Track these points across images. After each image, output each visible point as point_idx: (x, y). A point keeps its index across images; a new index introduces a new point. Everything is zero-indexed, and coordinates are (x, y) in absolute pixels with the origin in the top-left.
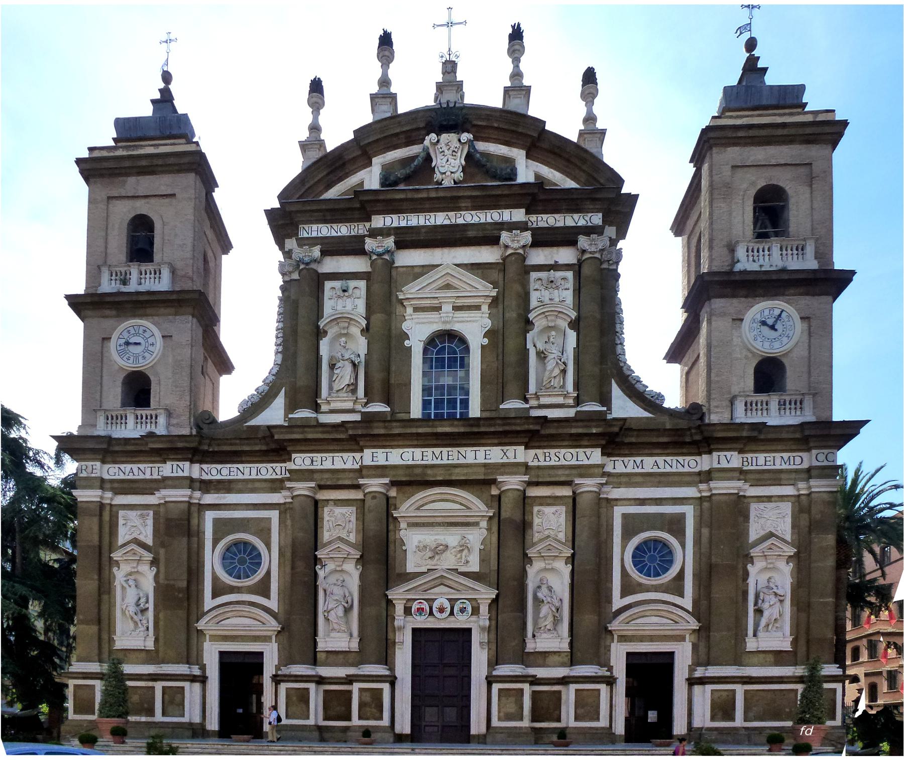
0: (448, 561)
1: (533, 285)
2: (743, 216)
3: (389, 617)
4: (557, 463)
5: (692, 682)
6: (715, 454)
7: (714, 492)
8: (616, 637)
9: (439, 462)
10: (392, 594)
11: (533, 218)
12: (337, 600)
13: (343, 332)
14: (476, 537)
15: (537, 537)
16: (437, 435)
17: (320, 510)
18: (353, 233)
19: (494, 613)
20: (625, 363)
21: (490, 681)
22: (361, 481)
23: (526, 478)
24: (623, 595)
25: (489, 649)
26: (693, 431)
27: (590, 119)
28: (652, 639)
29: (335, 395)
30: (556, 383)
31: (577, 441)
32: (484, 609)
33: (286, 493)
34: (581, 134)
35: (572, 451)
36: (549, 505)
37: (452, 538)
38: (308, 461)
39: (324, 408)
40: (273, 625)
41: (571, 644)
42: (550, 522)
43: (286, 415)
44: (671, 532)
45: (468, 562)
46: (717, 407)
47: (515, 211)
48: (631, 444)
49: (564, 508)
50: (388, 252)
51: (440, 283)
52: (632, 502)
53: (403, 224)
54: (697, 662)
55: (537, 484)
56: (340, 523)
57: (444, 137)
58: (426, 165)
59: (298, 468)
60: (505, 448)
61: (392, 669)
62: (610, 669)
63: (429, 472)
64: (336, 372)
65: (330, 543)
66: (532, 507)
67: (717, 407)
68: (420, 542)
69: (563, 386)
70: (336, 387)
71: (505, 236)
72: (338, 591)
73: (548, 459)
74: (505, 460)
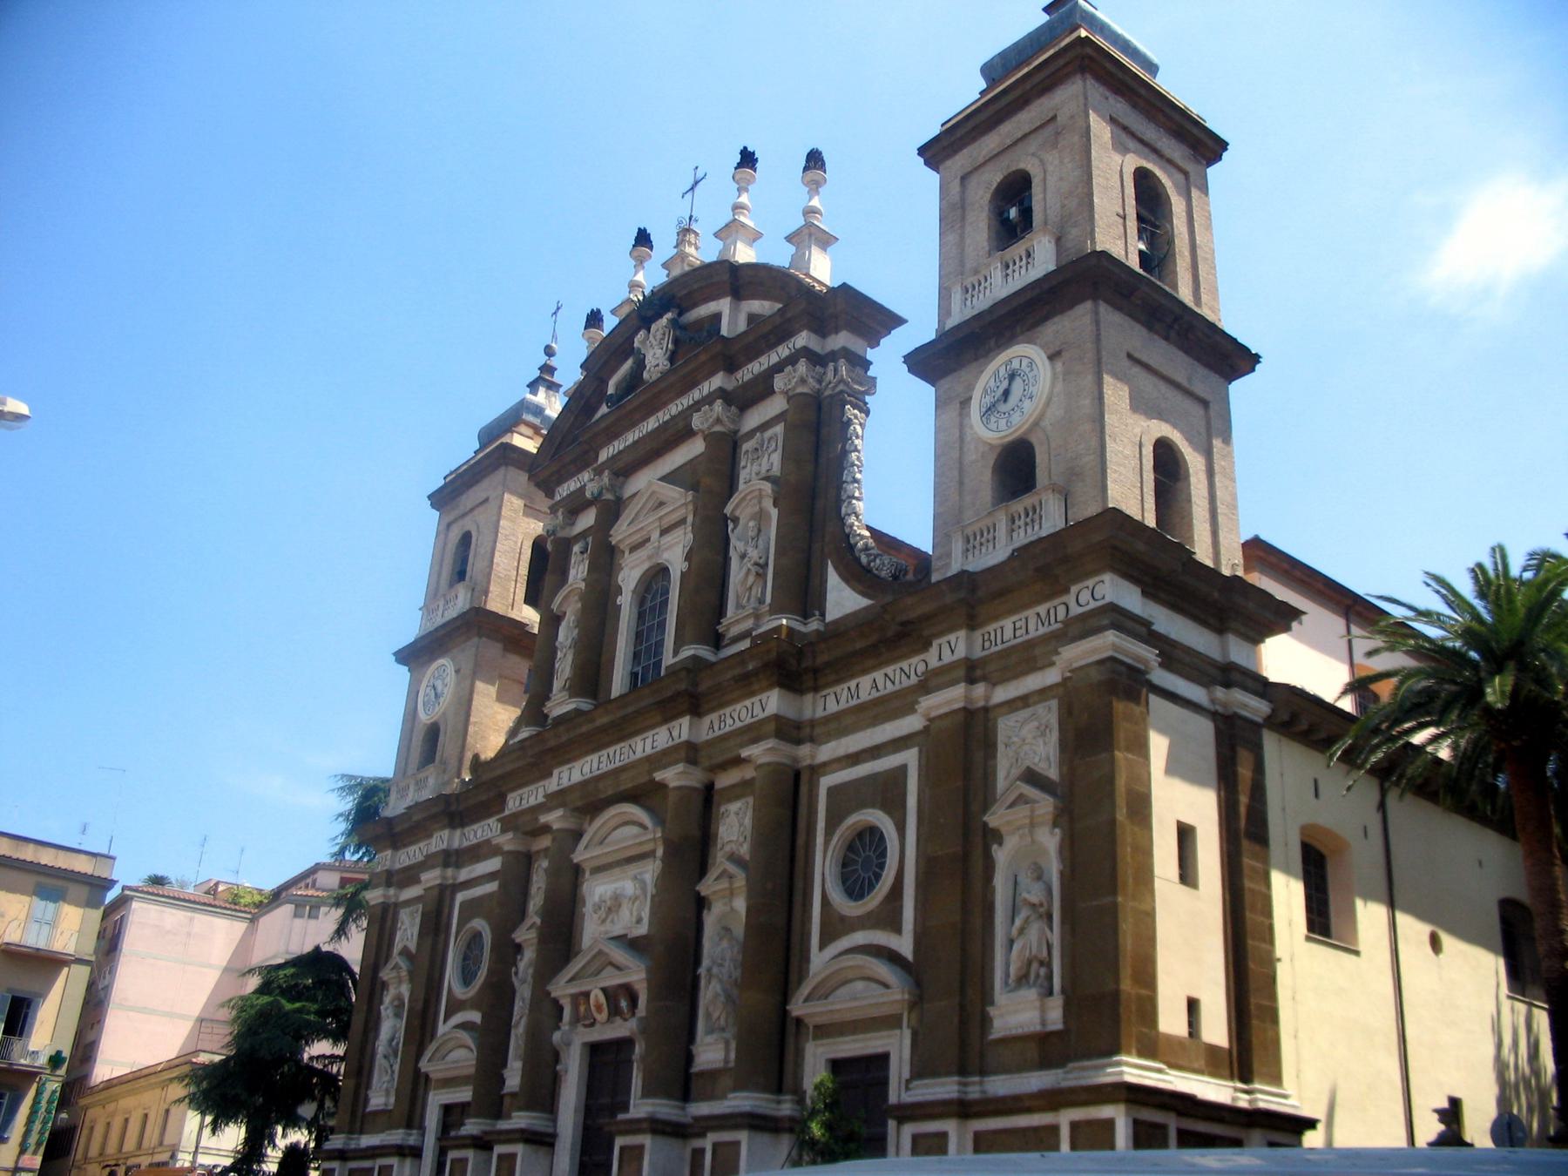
11: (739, 374)
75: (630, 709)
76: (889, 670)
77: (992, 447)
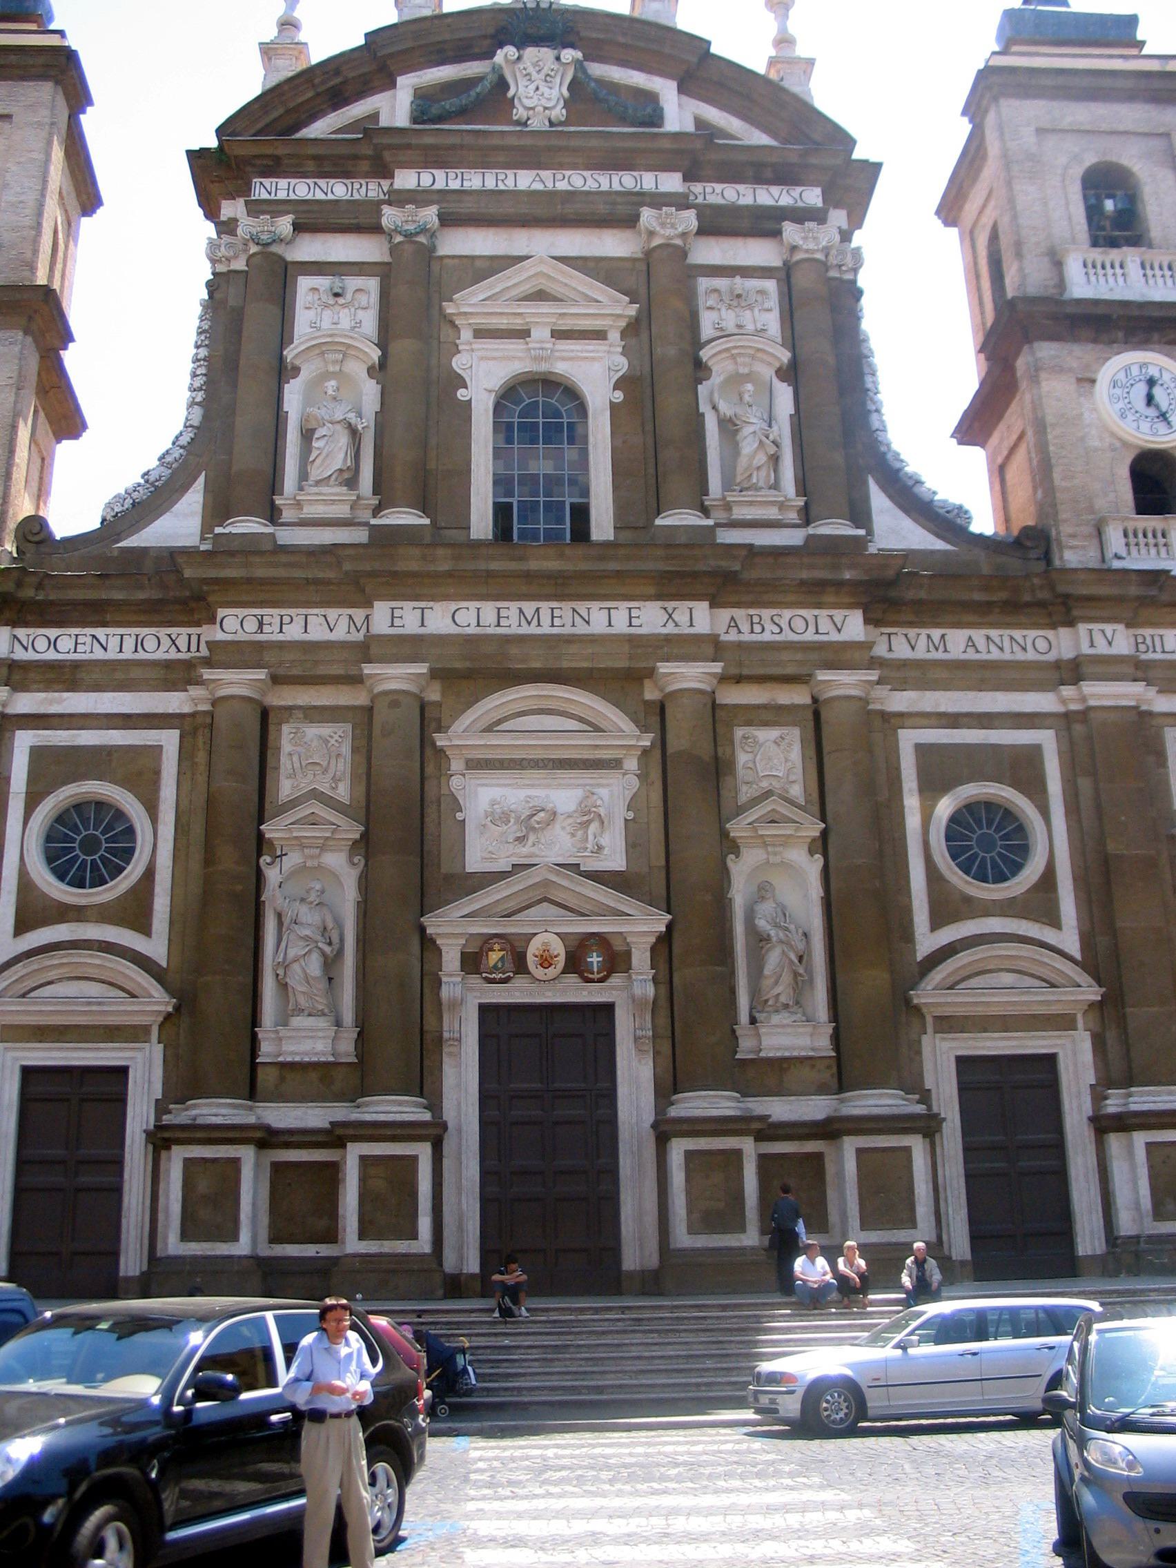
0: (558, 845)
1: (703, 301)
2: (1065, 212)
3: (431, 979)
4: (778, 638)
5: (1105, 1125)
6: (1083, 628)
7: (1092, 703)
8: (929, 1021)
9: (533, 630)
10: (435, 924)
11: (697, 188)
12: (306, 938)
13: (331, 369)
14: (615, 793)
15: (746, 793)
16: (528, 576)
17: (272, 728)
18: (356, 196)
19: (663, 967)
20: (888, 445)
21: (664, 1132)
22: (368, 669)
23: (717, 668)
24: (937, 922)
25: (656, 1054)
26: (1036, 581)
27: (784, 40)
28: (1006, 1023)
29: (315, 490)
30: (760, 478)
31: (815, 593)
32: (641, 959)
33: (195, 691)
34: (772, 62)
35: (808, 613)
36: (766, 724)
37: (564, 795)
38: (251, 625)
39: (288, 515)
40: (157, 1001)
41: (836, 1038)
42: (771, 759)
43: (206, 527)
44: (1016, 784)
45: (600, 848)
46: (1073, 536)
47: (663, 176)
48: (920, 602)
49: (795, 733)
50: (423, 230)
51: (527, 288)
52: (933, 721)
53: (455, 185)
54: (1106, 1081)
55: (739, 680)
56: (314, 761)
57: (531, 53)
58: (496, 97)
59: (229, 637)
60: (671, 605)
61: (435, 1105)
62: (925, 1097)
63: (514, 651)
64: (315, 444)
65: (293, 803)
66: (730, 726)
67: (1073, 536)
68: (493, 803)
69: (776, 486)
70: (315, 473)
71: (647, 216)
72: (310, 917)
73: (757, 628)
74: (670, 629)
75: (613, 566)
76: (994, 633)
77: (1126, 444)
